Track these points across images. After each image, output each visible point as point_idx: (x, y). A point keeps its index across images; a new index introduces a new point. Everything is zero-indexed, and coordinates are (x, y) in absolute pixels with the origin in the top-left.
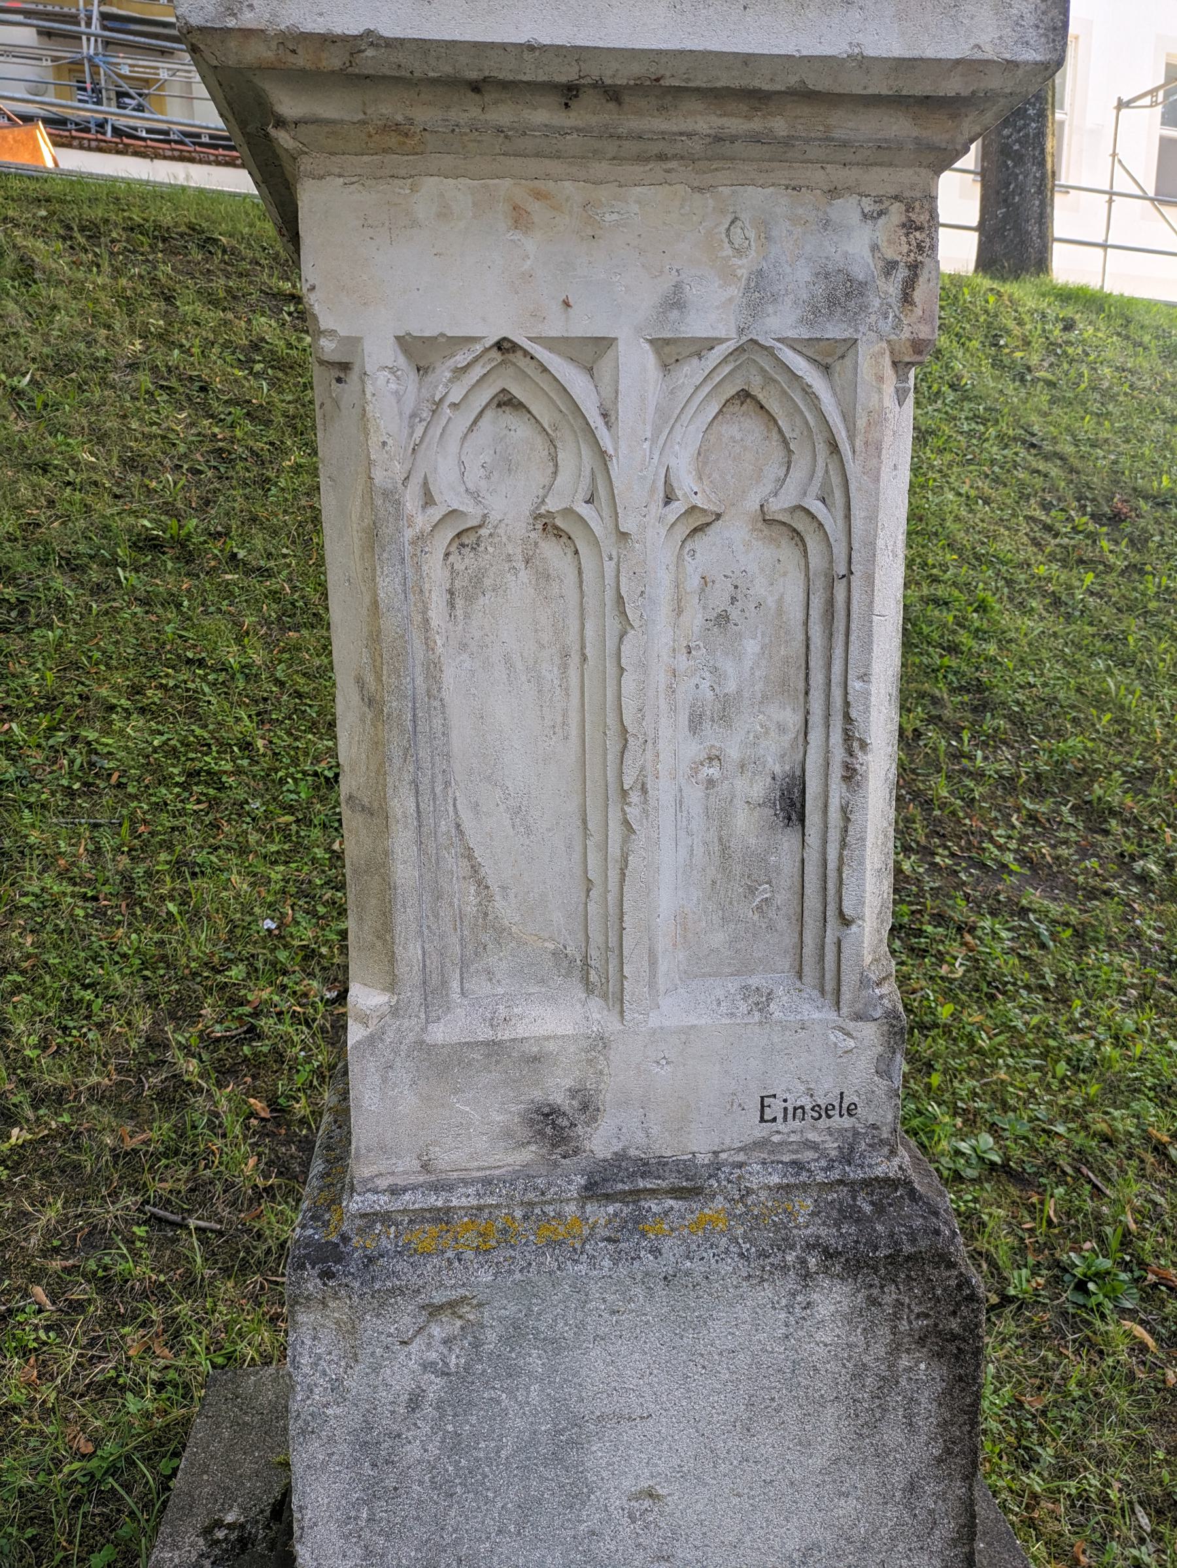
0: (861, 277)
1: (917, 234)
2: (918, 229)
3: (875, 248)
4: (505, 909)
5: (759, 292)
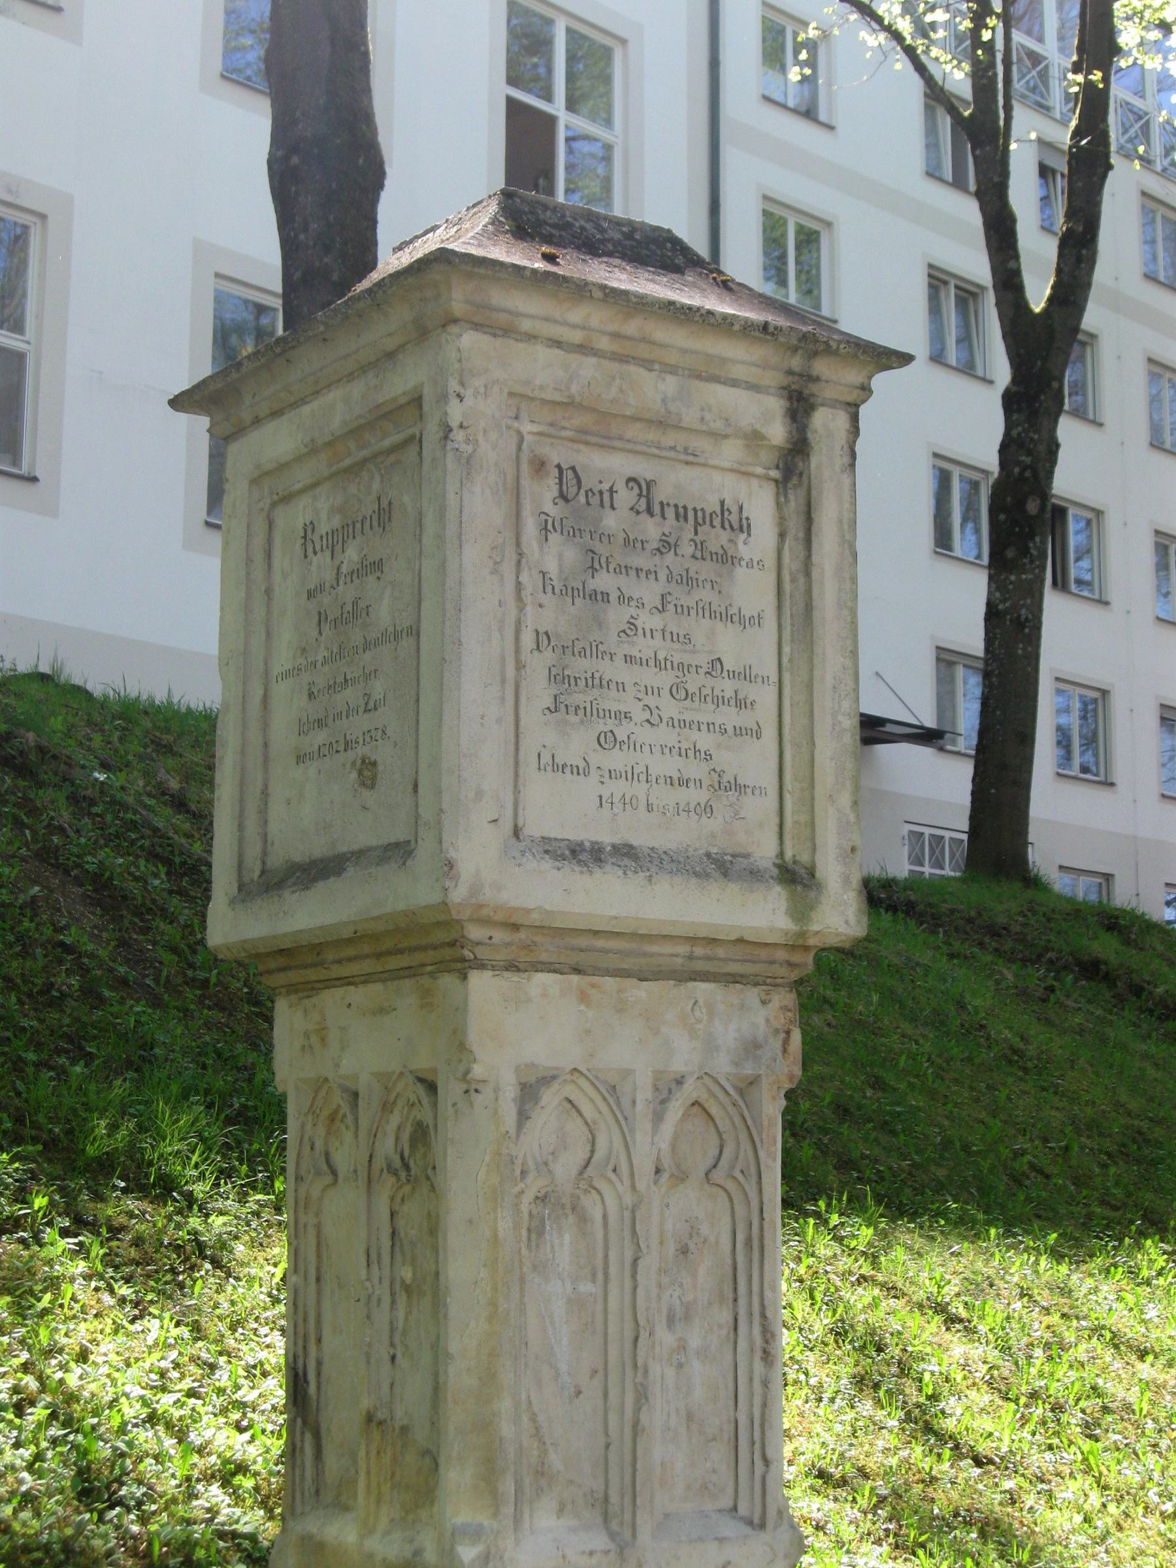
3: (767, 1020)
4: (555, 1460)
5: (710, 1046)
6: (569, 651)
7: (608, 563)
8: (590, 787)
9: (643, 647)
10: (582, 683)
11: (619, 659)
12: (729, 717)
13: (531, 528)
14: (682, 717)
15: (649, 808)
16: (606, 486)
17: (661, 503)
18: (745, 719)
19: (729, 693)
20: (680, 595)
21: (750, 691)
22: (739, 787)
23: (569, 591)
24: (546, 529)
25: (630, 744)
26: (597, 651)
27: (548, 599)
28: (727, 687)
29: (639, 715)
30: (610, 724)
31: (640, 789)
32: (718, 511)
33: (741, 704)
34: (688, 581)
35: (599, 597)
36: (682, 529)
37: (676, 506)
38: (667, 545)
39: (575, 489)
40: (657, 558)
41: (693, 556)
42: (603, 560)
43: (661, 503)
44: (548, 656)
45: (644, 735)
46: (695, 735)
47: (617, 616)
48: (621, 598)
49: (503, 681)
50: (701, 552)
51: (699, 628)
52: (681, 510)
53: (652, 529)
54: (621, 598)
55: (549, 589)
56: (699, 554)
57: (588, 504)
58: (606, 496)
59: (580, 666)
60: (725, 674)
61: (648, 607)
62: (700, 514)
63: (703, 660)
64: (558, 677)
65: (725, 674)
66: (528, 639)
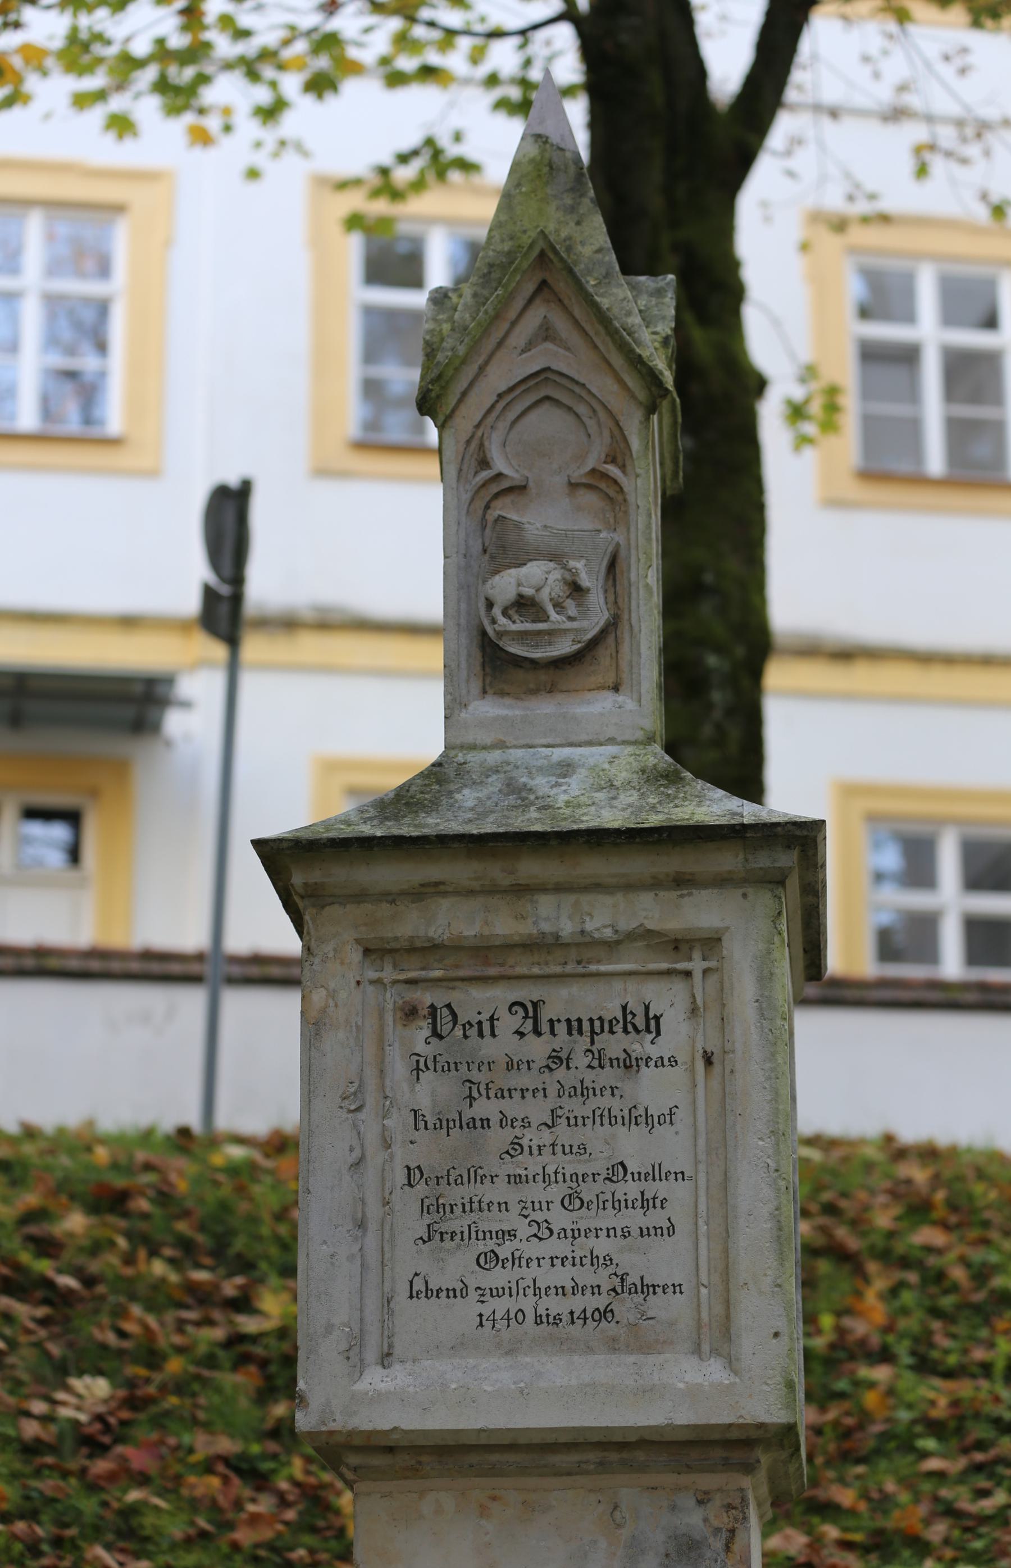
0: (698, 1538)
1: (733, 1511)
2: (733, 1508)
3: (706, 1520)
7: (487, 1089)
8: (469, 1308)
9: (533, 1165)
11: (501, 1182)
12: (635, 1219)
14: (575, 1227)
15: (538, 1320)
16: (485, 1017)
17: (551, 1021)
18: (656, 1218)
20: (575, 1107)
21: (660, 1189)
22: (648, 1289)
23: (443, 1124)
24: (418, 1069)
25: (515, 1260)
26: (476, 1175)
27: (420, 1135)
28: (631, 1189)
29: (524, 1230)
30: (491, 1244)
31: (528, 1304)
32: (620, 1016)
33: (646, 1203)
34: (583, 1091)
35: (478, 1124)
36: (575, 1042)
37: (568, 1021)
38: (557, 1059)
39: (451, 1025)
41: (589, 1066)
42: (482, 1088)
43: (551, 1021)
44: (421, 1189)
45: (533, 1249)
46: (592, 1242)
47: (499, 1138)
50: (599, 1060)
51: (594, 1136)
52: (575, 1024)
53: (538, 1048)
55: (422, 1124)
56: (595, 1063)
57: (466, 1037)
58: (486, 1027)
59: (455, 1194)
60: (629, 1177)
61: (534, 1125)
62: (597, 1023)
63: (600, 1166)
64: (434, 1207)
65: (629, 1177)
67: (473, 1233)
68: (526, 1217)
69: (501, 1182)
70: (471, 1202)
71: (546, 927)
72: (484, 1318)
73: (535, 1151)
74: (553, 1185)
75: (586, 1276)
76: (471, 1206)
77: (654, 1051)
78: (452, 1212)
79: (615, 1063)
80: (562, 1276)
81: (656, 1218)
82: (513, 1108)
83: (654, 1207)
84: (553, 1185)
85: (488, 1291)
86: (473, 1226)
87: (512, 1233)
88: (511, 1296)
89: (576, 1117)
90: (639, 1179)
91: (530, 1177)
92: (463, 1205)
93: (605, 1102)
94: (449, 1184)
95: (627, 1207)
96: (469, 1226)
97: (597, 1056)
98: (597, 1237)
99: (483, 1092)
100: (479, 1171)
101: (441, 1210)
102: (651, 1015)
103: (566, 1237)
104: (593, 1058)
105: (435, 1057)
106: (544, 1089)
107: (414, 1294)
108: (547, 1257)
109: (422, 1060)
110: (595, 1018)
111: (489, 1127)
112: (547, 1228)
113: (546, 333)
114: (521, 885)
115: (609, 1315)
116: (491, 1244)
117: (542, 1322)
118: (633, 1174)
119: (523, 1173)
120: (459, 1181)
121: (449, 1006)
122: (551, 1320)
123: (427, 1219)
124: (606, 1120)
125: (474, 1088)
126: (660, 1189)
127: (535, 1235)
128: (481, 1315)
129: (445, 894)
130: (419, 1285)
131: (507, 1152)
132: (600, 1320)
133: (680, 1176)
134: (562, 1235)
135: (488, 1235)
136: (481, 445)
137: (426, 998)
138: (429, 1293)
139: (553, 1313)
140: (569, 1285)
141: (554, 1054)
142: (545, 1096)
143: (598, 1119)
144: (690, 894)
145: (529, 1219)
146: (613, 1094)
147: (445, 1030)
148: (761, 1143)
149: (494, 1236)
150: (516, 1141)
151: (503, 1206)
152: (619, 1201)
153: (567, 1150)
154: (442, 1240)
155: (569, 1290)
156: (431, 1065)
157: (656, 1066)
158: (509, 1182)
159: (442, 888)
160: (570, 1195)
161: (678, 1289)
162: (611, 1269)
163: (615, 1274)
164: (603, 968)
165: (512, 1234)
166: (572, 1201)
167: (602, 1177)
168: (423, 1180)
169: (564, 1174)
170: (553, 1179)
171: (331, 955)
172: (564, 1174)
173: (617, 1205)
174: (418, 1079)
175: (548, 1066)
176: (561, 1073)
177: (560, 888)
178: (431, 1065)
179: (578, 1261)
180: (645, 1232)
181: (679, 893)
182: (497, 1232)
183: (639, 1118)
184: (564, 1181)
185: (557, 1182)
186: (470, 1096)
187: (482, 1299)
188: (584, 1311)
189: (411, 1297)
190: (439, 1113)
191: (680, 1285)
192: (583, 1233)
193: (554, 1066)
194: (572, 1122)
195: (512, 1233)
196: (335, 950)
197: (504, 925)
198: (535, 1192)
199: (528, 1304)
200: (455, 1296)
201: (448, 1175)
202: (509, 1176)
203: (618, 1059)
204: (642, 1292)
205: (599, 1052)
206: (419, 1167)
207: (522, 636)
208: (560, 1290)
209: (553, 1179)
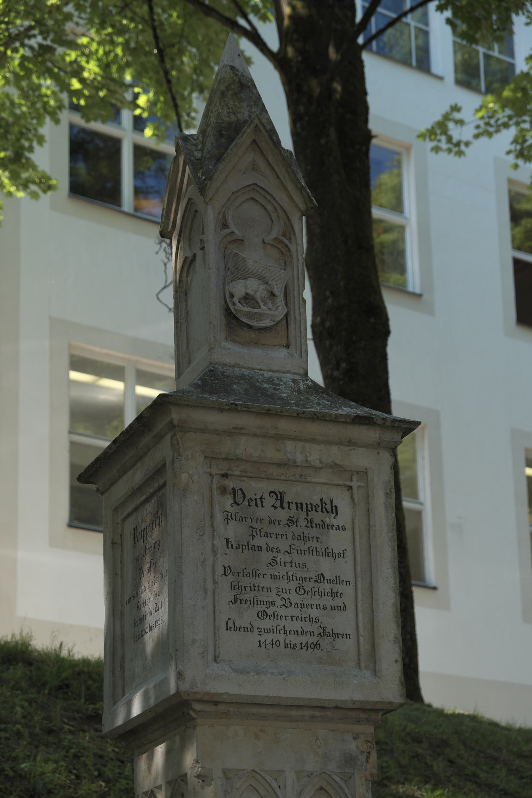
2: (369, 742)
3: (357, 747)
6: (241, 575)
7: (260, 532)
8: (255, 637)
9: (281, 571)
10: (248, 589)
11: (268, 577)
12: (328, 601)
13: (219, 518)
14: (302, 603)
16: (258, 497)
17: (288, 502)
18: (338, 602)
19: (328, 590)
20: (301, 545)
21: (339, 588)
22: (335, 635)
24: (227, 519)
25: (275, 616)
26: (256, 574)
28: (326, 587)
29: (279, 602)
30: (264, 607)
31: (281, 637)
33: (334, 594)
34: (304, 538)
35: (256, 548)
37: (296, 503)
38: (292, 521)
39: (242, 498)
40: (287, 528)
41: (306, 526)
42: (258, 531)
43: (288, 502)
44: (230, 577)
45: (282, 612)
46: (309, 610)
47: (266, 556)
48: (269, 548)
49: (206, 591)
50: (310, 524)
52: (299, 505)
53: (283, 515)
54: (269, 548)
55: (230, 546)
56: (309, 525)
57: (249, 505)
59: (246, 582)
60: (325, 581)
61: (282, 552)
62: (309, 506)
63: (312, 575)
65: (325, 581)
66: (220, 570)
67: (255, 602)
68: (279, 596)
69: (268, 577)
70: (254, 586)
71: (290, 456)
72: (261, 643)
73: (283, 565)
74: (291, 582)
75: (308, 627)
76: (254, 588)
77: (335, 522)
78: (245, 590)
79: (318, 526)
80: (297, 626)
81: (338, 602)
82: (273, 542)
83: (337, 596)
84: (291, 582)
85: (263, 630)
86: (255, 598)
87: (273, 603)
88: (273, 633)
89: (301, 550)
90: (330, 583)
91: (281, 577)
92: (251, 587)
93: (314, 544)
94: (244, 576)
95: (325, 595)
96: (254, 598)
97: (309, 522)
98: (312, 608)
99: (258, 533)
100: (257, 571)
101: (240, 588)
102: (334, 505)
103: (298, 607)
104: (308, 522)
105: (235, 514)
106: (286, 535)
107: (229, 628)
108: (290, 616)
109: (229, 514)
110: (308, 503)
111: (261, 551)
112: (289, 602)
113: (254, 167)
114: (278, 434)
115: (318, 646)
116: (264, 607)
117: (288, 647)
118: (327, 580)
119: (278, 574)
120: (248, 575)
121: (241, 489)
122: (292, 646)
123: (234, 593)
124: (314, 553)
125: (254, 531)
126: (339, 588)
127: (284, 605)
128: (260, 641)
129: (243, 434)
130: (230, 624)
131: (270, 564)
132: (314, 648)
133: (348, 583)
134: (296, 606)
135: (262, 603)
136: (224, 216)
137: (230, 484)
138: (235, 628)
139: (293, 643)
140: (300, 630)
141: (290, 518)
142: (287, 538)
143: (311, 552)
144: (354, 449)
145: (281, 597)
146: (317, 541)
147: (240, 501)
148: (388, 571)
149: (265, 604)
150: (274, 558)
151: (269, 590)
152: (321, 592)
153: (297, 565)
154: (241, 603)
155: (300, 633)
156: (234, 517)
157: (336, 529)
158: (271, 578)
159: (243, 431)
160: (299, 587)
161: (348, 636)
162: (319, 624)
163: (320, 627)
164: (313, 480)
165: (273, 604)
166: (300, 590)
167: (313, 580)
168: (231, 573)
169: (296, 577)
170: (291, 578)
171: (190, 457)
172: (296, 577)
173: (320, 593)
174: (228, 523)
175: (287, 524)
176: (293, 528)
177: (296, 439)
178: (234, 517)
179: (303, 619)
180: (333, 608)
181: (349, 448)
182: (266, 602)
183: (329, 553)
184: (296, 580)
185: (293, 580)
186: (252, 535)
187: (260, 633)
188: (307, 643)
189: (227, 630)
190: (238, 541)
191: (349, 635)
192: (305, 606)
193: (290, 524)
194: (299, 552)
195: (273, 603)
196: (192, 455)
197: (271, 453)
198: (284, 584)
199: (281, 637)
200: (248, 631)
201: (243, 572)
202: (271, 575)
203: (319, 524)
204: (333, 636)
205: (311, 520)
206: (229, 567)
207: (248, 315)
208: (296, 632)
209: (291, 578)
